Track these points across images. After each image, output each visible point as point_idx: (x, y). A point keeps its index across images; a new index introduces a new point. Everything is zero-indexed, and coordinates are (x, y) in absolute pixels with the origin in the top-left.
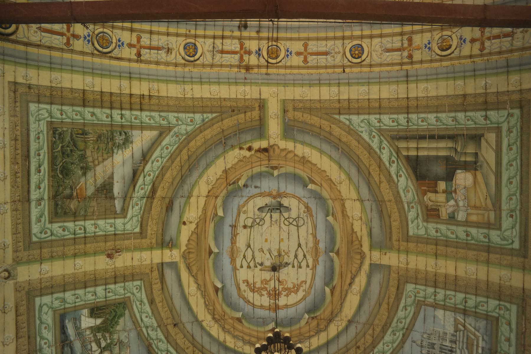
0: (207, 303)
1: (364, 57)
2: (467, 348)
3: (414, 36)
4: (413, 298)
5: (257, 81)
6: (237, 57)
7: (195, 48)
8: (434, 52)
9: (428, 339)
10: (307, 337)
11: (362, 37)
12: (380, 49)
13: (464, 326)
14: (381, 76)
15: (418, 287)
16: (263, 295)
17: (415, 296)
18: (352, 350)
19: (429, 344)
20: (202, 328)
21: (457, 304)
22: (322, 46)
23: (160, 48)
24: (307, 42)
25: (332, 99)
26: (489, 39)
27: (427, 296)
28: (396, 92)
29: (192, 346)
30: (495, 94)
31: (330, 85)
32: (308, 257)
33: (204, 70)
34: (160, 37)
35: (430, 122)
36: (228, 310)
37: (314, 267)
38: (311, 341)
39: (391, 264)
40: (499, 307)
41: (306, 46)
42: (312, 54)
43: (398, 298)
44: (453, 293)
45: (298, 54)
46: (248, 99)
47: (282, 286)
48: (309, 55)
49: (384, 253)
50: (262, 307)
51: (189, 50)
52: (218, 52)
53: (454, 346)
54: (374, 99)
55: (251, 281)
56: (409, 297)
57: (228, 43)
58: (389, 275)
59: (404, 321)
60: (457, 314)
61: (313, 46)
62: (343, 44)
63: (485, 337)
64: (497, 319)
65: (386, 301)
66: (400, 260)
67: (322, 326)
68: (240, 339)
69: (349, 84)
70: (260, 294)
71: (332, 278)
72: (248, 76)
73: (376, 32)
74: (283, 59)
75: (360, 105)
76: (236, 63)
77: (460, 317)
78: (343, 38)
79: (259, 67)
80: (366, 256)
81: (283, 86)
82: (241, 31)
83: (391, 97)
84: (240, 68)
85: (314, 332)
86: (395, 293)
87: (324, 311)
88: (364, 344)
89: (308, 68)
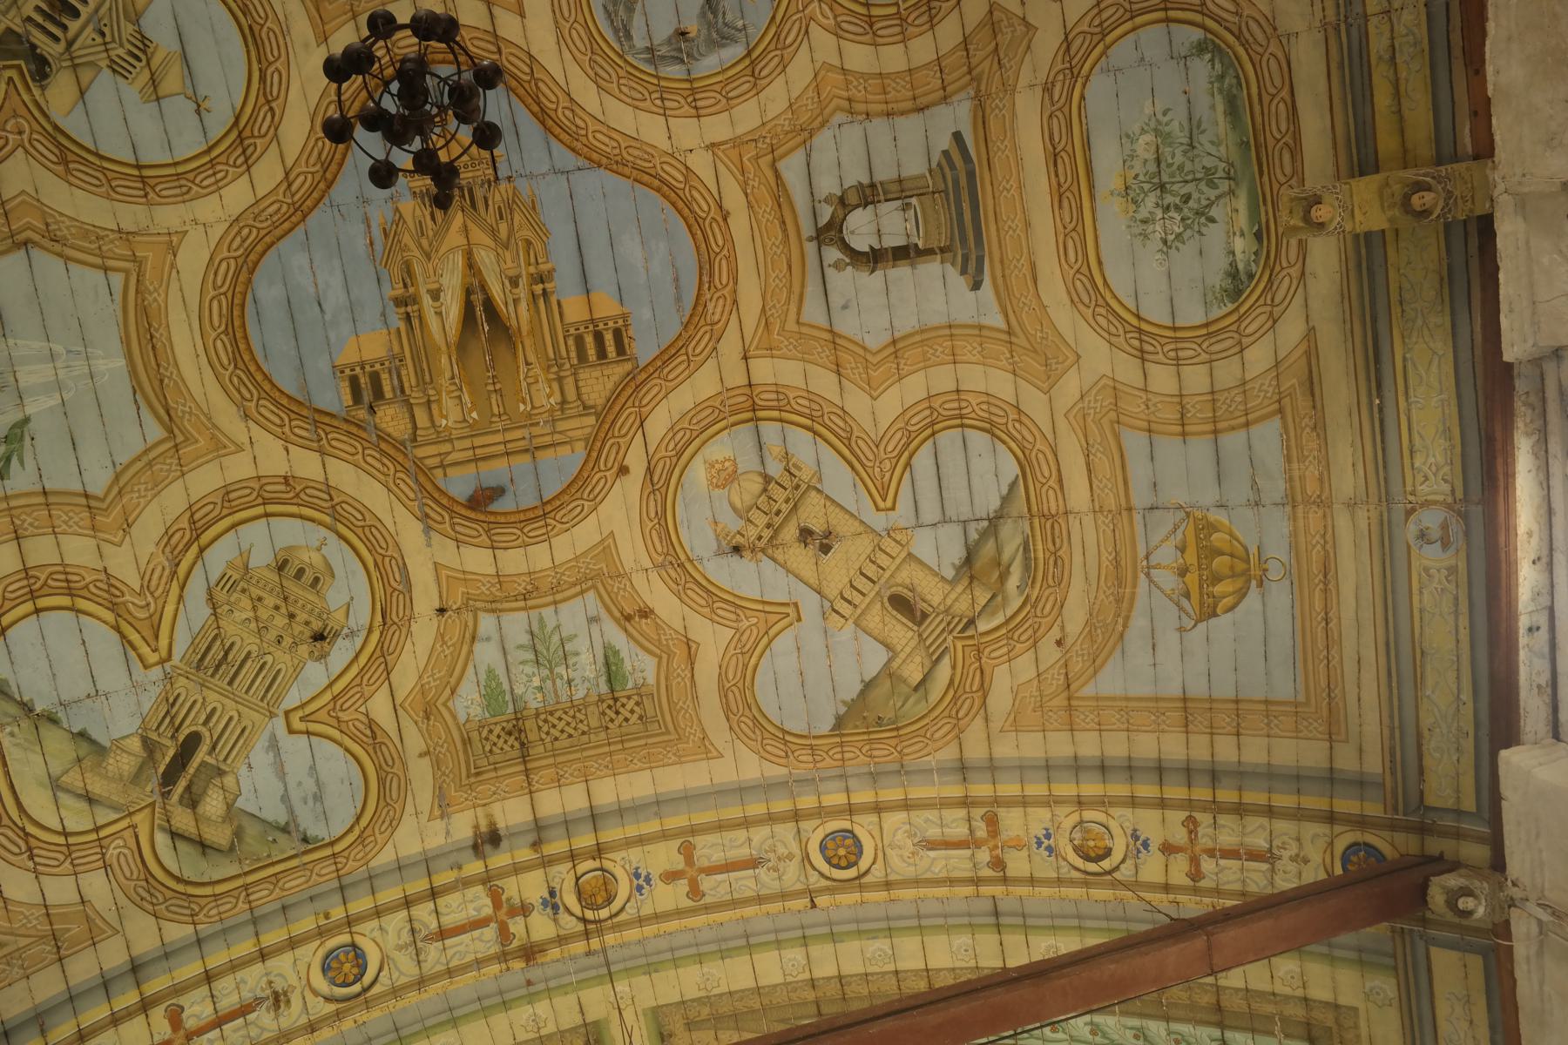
1: (864, 864)
3: (1002, 812)
5: (565, 980)
6: (490, 932)
7: (357, 956)
8: (1065, 859)
11: (851, 810)
12: (909, 843)
14: (922, 912)
22: (736, 845)
23: (250, 1004)
24: (691, 839)
25: (791, 979)
26: (1211, 853)
28: (971, 952)
30: (1241, 994)
31: (778, 944)
33: (401, 1004)
34: (239, 975)
35: (1074, 1033)
41: (687, 851)
42: (710, 871)
45: (671, 877)
46: (550, 1036)
48: (703, 875)
51: (340, 969)
52: (429, 938)
54: (912, 971)
57: (455, 905)
61: (709, 849)
62: (799, 832)
69: (833, 937)
72: (535, 973)
73: (892, 794)
74: (628, 901)
75: (874, 989)
76: (492, 951)
78: (796, 816)
79: (561, 940)
81: (644, 974)
82: (483, 857)
83: (958, 964)
84: (506, 961)
89: (708, 909)
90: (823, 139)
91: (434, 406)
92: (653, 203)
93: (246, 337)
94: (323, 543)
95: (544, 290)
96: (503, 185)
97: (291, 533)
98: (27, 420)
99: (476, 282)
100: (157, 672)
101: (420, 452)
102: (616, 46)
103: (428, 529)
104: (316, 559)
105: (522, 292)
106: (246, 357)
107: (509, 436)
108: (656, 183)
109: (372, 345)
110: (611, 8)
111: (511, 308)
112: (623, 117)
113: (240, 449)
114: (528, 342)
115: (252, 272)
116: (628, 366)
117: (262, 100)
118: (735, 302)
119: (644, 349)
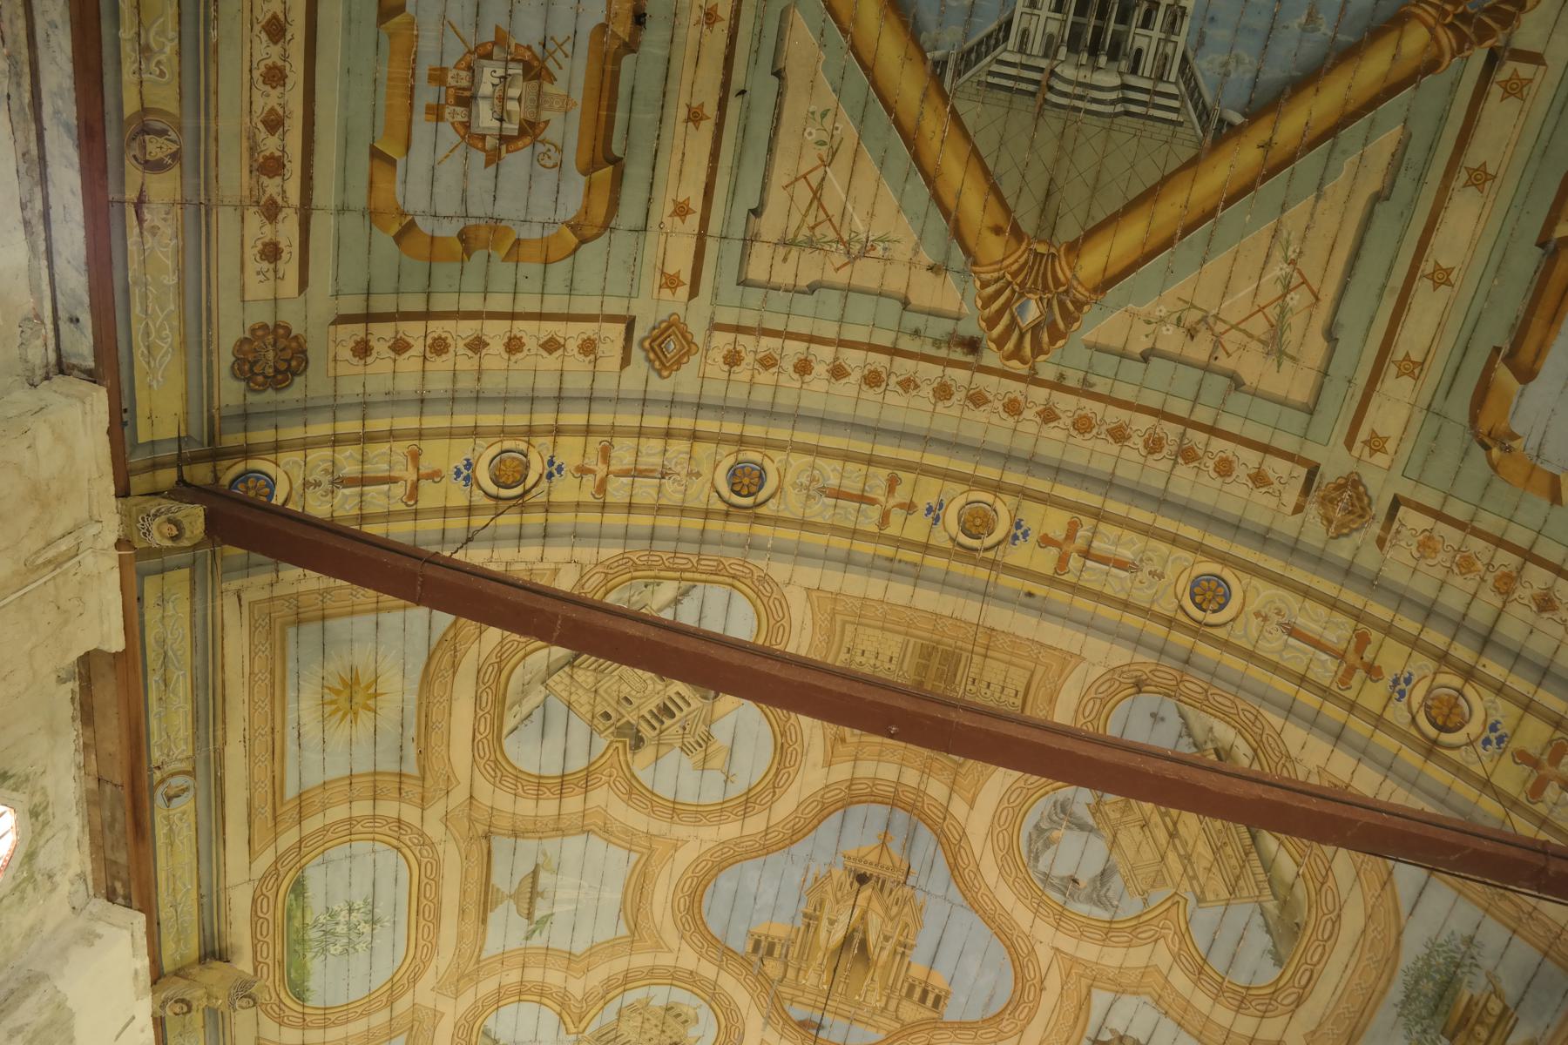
90: (1128, 1004)
91: (802, 973)
92: (998, 950)
93: (700, 902)
94: (700, 1007)
95: (903, 953)
96: (907, 889)
97: (681, 997)
98: (552, 914)
99: (861, 927)
100: (573, 1037)
101: (781, 989)
102: (1025, 860)
103: (766, 1023)
104: (691, 1012)
105: (889, 946)
106: (696, 911)
107: (841, 1006)
108: (1008, 943)
109: (779, 928)
110: (1034, 837)
111: (877, 950)
112: (1007, 898)
113: (670, 951)
114: (878, 971)
115: (720, 871)
116: (936, 1016)
117: (771, 786)
118: (1022, 1031)
119: (951, 1013)
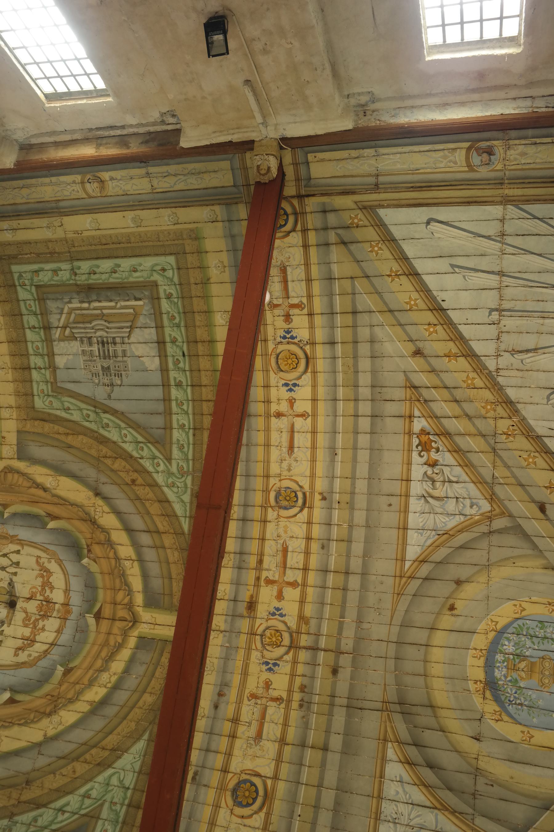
0: (23, 721)
2: (90, 322)
4: (51, 399)
9: (99, 376)
10: (116, 563)
13: (64, 327)
15: (35, 393)
16: (44, 626)
17: (48, 396)
18: (138, 493)
19: (105, 374)
20: (55, 738)
21: (41, 338)
27: (44, 380)
29: (75, 764)
32: (5, 551)
36: (47, 688)
37: (21, 542)
38: (123, 557)
39: (15, 430)
40: (23, 285)
43: (57, 420)
44: (29, 345)
47: (38, 595)
49: (3, 440)
50: (59, 631)
53: (95, 340)
55: (19, 643)
56: (52, 405)
58: (29, 432)
59: (85, 412)
60: (53, 337)
63: (67, 300)
64: (37, 287)
65: (63, 438)
66: (9, 418)
67: (102, 537)
68: (97, 677)
70: (40, 631)
71: (36, 517)
77: (55, 333)
80: (8, 466)
85: (110, 551)
86: (51, 425)
87: (81, 532)
88: (128, 472)
